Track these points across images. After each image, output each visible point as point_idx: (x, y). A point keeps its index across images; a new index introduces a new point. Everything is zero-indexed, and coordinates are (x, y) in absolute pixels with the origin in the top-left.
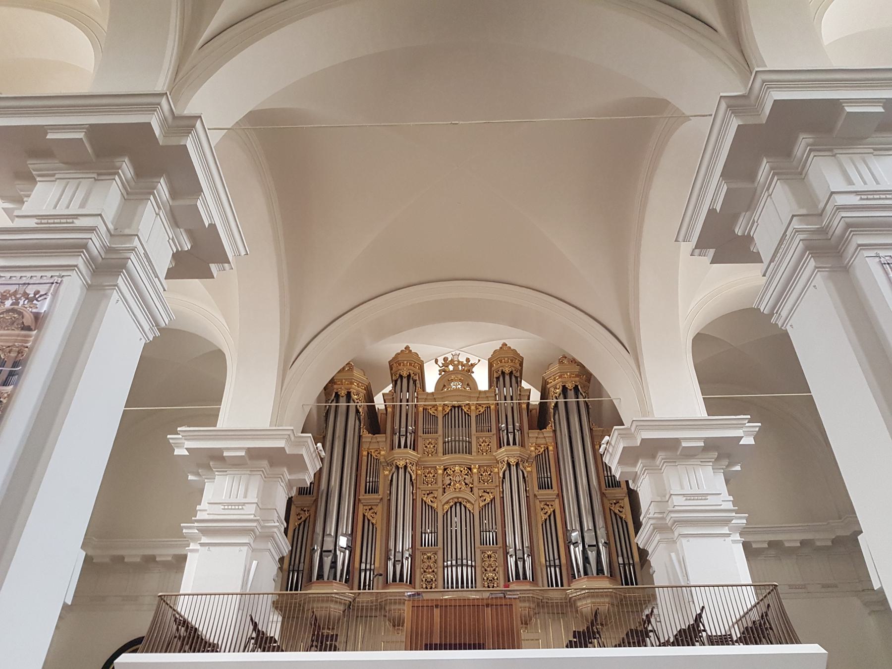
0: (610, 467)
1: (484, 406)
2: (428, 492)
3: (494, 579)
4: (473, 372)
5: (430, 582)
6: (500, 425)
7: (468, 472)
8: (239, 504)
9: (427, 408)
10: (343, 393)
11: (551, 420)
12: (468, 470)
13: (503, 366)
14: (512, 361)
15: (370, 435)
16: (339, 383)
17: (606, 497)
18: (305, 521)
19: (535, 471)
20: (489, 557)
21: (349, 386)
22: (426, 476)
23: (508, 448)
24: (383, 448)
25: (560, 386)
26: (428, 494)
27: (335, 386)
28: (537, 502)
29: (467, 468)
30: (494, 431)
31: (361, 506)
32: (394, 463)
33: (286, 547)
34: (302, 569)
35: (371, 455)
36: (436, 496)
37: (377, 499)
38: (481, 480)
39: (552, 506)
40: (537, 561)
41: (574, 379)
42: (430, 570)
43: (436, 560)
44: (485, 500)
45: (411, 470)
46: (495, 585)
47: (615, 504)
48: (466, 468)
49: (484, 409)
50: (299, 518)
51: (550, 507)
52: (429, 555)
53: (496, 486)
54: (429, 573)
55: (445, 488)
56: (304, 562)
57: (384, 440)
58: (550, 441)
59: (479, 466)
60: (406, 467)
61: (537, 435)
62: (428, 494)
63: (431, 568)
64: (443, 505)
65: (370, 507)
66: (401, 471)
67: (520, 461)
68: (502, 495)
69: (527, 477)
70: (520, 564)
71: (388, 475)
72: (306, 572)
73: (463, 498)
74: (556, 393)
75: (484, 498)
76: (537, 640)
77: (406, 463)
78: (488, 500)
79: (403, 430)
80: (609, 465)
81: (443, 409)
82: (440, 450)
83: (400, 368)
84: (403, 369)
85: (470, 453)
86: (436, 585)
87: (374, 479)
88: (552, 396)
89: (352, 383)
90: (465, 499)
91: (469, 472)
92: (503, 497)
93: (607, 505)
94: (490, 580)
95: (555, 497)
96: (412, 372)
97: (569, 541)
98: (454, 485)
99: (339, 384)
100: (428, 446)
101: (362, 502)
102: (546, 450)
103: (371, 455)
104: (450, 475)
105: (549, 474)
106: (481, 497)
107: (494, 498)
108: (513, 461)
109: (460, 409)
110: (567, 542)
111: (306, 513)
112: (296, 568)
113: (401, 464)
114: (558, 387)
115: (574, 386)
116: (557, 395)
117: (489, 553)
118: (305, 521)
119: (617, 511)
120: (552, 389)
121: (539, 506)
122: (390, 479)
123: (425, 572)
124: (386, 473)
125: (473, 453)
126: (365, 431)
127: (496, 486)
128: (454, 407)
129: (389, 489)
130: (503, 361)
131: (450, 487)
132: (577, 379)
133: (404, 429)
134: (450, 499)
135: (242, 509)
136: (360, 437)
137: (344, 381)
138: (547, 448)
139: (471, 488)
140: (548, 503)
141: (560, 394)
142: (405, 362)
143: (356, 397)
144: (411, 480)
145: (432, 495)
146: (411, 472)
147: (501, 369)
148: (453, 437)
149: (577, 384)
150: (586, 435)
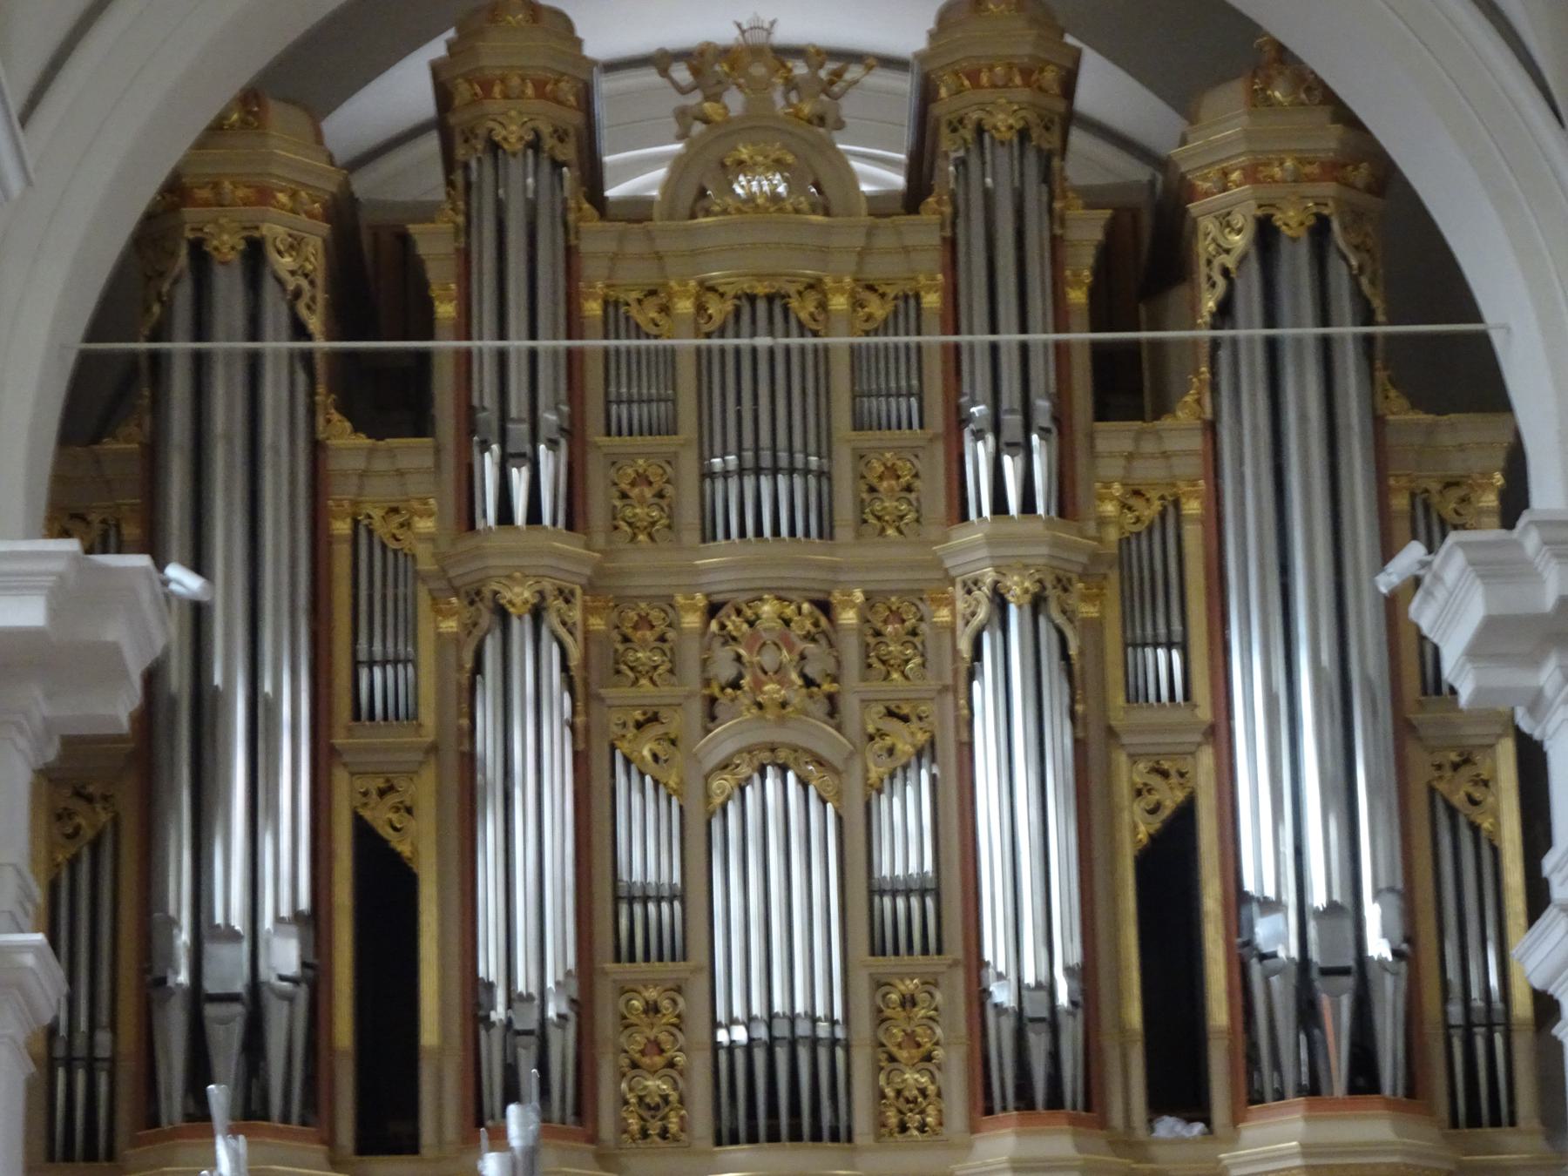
0: (1436, 650)
1: (891, 292)
2: (638, 715)
3: (923, 1092)
4: (840, 125)
5: (657, 1108)
6: (964, 400)
9: (623, 297)
10: (227, 244)
11: (1197, 373)
12: (818, 613)
13: (981, 106)
14: (1026, 73)
15: (363, 441)
16: (205, 194)
17: (1420, 739)
20: (909, 1002)
21: (250, 213)
23: (1003, 527)
24: (424, 501)
25: (1244, 217)
26: (639, 725)
27: (190, 214)
28: (1122, 759)
30: (937, 418)
32: (487, 593)
39: (1182, 775)
41: (1307, 189)
43: (678, 1016)
44: (891, 751)
45: (564, 624)
46: (929, 1120)
47: (1456, 767)
48: (806, 607)
49: (889, 307)
50: (69, 830)
51: (1174, 780)
52: (652, 994)
54: (654, 1072)
55: (713, 700)
57: (429, 462)
58: (1191, 467)
59: (865, 593)
60: (537, 614)
61: (1127, 445)
62: (639, 725)
64: (707, 777)
65: (381, 783)
66: (521, 630)
67: (1049, 585)
68: (965, 737)
69: (1081, 653)
70: (1010, 466)
71: (457, 641)
72: (128, 1069)
73: (795, 749)
74: (1228, 251)
75: (888, 741)
78: (905, 748)
79: (519, 431)
80: (1435, 637)
81: (701, 308)
82: (689, 514)
83: (495, 105)
85: (826, 531)
86: (682, 1118)
87: (390, 644)
88: (1209, 262)
89: (264, 196)
91: (823, 621)
92: (971, 745)
93: (1422, 773)
95: (1198, 738)
96: (546, 130)
97: (1245, 938)
98: (758, 685)
99: (207, 204)
100: (635, 492)
101: (347, 758)
103: (370, 532)
106: (871, 738)
107: (932, 744)
108: (1017, 587)
110: (1239, 940)
111: (98, 807)
113: (517, 601)
114: (1238, 220)
115: (1311, 221)
116: (1230, 261)
117: (911, 985)
118: (95, 846)
119: (1458, 799)
120: (1208, 225)
121: (1127, 774)
122: (469, 665)
123: (635, 1065)
124: (450, 625)
125: (838, 532)
126: (336, 416)
127: (945, 689)
128: (752, 299)
130: (984, 79)
131: (733, 700)
132: (1329, 189)
134: (739, 752)
136: (317, 448)
137: (227, 186)
138: (1177, 504)
139: (831, 698)
140: (1166, 765)
141: (1243, 259)
143: (287, 260)
144: (565, 667)
145: (656, 730)
146: (562, 632)
147: (975, 116)
148: (748, 455)
149: (1326, 212)
150: (1349, 427)
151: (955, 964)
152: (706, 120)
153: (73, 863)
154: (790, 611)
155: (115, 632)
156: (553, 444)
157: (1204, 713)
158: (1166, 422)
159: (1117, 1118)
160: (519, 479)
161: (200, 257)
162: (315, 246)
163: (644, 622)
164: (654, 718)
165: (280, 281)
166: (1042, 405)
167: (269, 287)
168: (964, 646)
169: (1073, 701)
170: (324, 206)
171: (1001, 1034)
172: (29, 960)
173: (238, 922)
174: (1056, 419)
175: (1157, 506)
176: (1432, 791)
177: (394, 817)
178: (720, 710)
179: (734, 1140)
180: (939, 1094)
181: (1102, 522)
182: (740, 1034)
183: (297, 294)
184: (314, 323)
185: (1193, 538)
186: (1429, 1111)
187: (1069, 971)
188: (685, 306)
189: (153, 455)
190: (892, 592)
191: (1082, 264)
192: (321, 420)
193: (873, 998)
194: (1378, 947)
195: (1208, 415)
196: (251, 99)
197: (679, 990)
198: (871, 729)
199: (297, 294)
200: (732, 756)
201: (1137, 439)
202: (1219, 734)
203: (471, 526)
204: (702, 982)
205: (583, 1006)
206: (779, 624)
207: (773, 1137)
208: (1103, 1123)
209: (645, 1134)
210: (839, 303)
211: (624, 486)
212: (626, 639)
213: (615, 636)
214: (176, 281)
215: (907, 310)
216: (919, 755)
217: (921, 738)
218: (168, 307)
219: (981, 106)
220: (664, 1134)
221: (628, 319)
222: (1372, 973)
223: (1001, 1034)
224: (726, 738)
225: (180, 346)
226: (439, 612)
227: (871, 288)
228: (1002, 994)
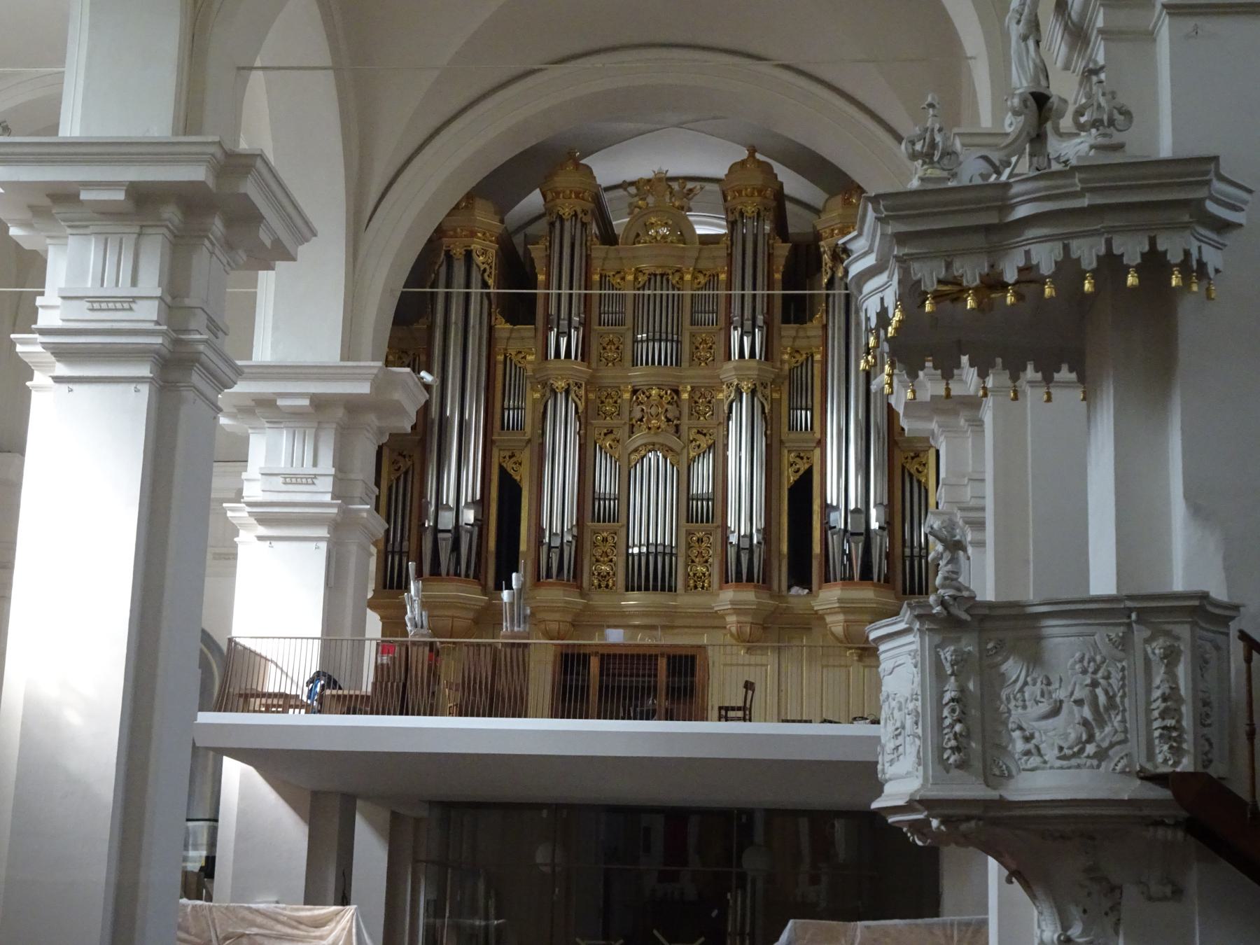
1: (708, 273)
3: (704, 574)
5: (605, 577)
7: (673, 398)
8: (307, 476)
9: (607, 274)
10: (458, 252)
13: (742, 203)
14: (760, 192)
15: (508, 326)
16: (451, 233)
17: (899, 448)
18: (406, 473)
19: (785, 397)
20: (700, 540)
22: (602, 402)
23: (742, 363)
26: (605, 434)
27: (445, 240)
29: (671, 390)
30: (722, 323)
31: (495, 452)
33: (379, 525)
34: (407, 550)
35: (511, 360)
36: (618, 437)
37: (521, 440)
38: (693, 412)
40: (773, 548)
42: (606, 559)
44: (699, 446)
45: (577, 396)
49: (707, 279)
52: (605, 534)
53: (720, 424)
54: (604, 563)
55: (633, 425)
56: (409, 540)
57: (532, 334)
58: (818, 342)
60: (567, 392)
61: (793, 333)
62: (605, 434)
63: (608, 556)
64: (630, 454)
66: (561, 398)
67: (757, 385)
75: (698, 443)
76: (762, 665)
77: (569, 384)
78: (704, 446)
79: (564, 323)
81: (636, 278)
82: (628, 356)
84: (564, 204)
89: (473, 234)
90: (666, 446)
91: (675, 397)
93: (899, 459)
94: (698, 577)
95: (815, 445)
96: (579, 211)
98: (649, 421)
99: (451, 237)
102: (810, 359)
103: (511, 360)
104: (642, 403)
105: (809, 402)
106: (692, 441)
107: (714, 443)
108: (746, 386)
109: (664, 279)
112: (397, 549)
113: (560, 387)
117: (701, 534)
118: (406, 473)
119: (913, 471)
121: (788, 457)
122: (542, 411)
123: (597, 561)
126: (499, 316)
128: (655, 275)
129: (540, 426)
130: (744, 193)
131: (640, 426)
133: (566, 322)
134: (641, 445)
135: (313, 483)
136: (491, 329)
137: (459, 230)
140: (802, 455)
142: (568, 192)
143: (481, 258)
145: (612, 436)
147: (739, 207)
148: (651, 334)
151: (718, 527)
152: (640, 208)
153: (398, 479)
154: (663, 393)
155: (397, 396)
156: (577, 329)
157: (818, 435)
158: (809, 324)
159: (775, 587)
160: (564, 342)
161: (449, 257)
162: (492, 252)
163: (609, 396)
164: (611, 432)
165: (478, 267)
166: (760, 319)
167: (474, 268)
168: (726, 408)
169: (766, 430)
170: (497, 238)
171: (732, 552)
172: (365, 515)
173: (452, 503)
174: (765, 322)
175: (804, 356)
176: (903, 468)
177: (514, 466)
178: (635, 429)
179: (633, 590)
180: (710, 575)
181: (782, 362)
182: (636, 550)
183: (485, 270)
184: (491, 282)
185: (817, 367)
186: (894, 589)
187: (758, 530)
188: (630, 278)
189: (431, 328)
190: (702, 387)
191: (780, 264)
192: (493, 319)
193: (686, 538)
194: (874, 525)
195: (825, 322)
196: (470, 197)
197: (616, 534)
198: (691, 439)
199: (485, 270)
200: (639, 447)
201: (797, 331)
202: (821, 443)
203: (547, 358)
204: (624, 530)
205: (578, 539)
206: (657, 398)
207: (655, 589)
208: (770, 588)
209: (600, 586)
210: (688, 277)
211: (605, 345)
212: (602, 402)
213: (598, 401)
214: (440, 266)
215: (712, 281)
216: (709, 448)
217: (710, 442)
218: (437, 275)
219: (742, 203)
220: (607, 586)
221: (609, 281)
222: (872, 535)
223: (732, 552)
224: (639, 438)
225: (441, 290)
226: (533, 389)
227: (700, 272)
228: (733, 539)
